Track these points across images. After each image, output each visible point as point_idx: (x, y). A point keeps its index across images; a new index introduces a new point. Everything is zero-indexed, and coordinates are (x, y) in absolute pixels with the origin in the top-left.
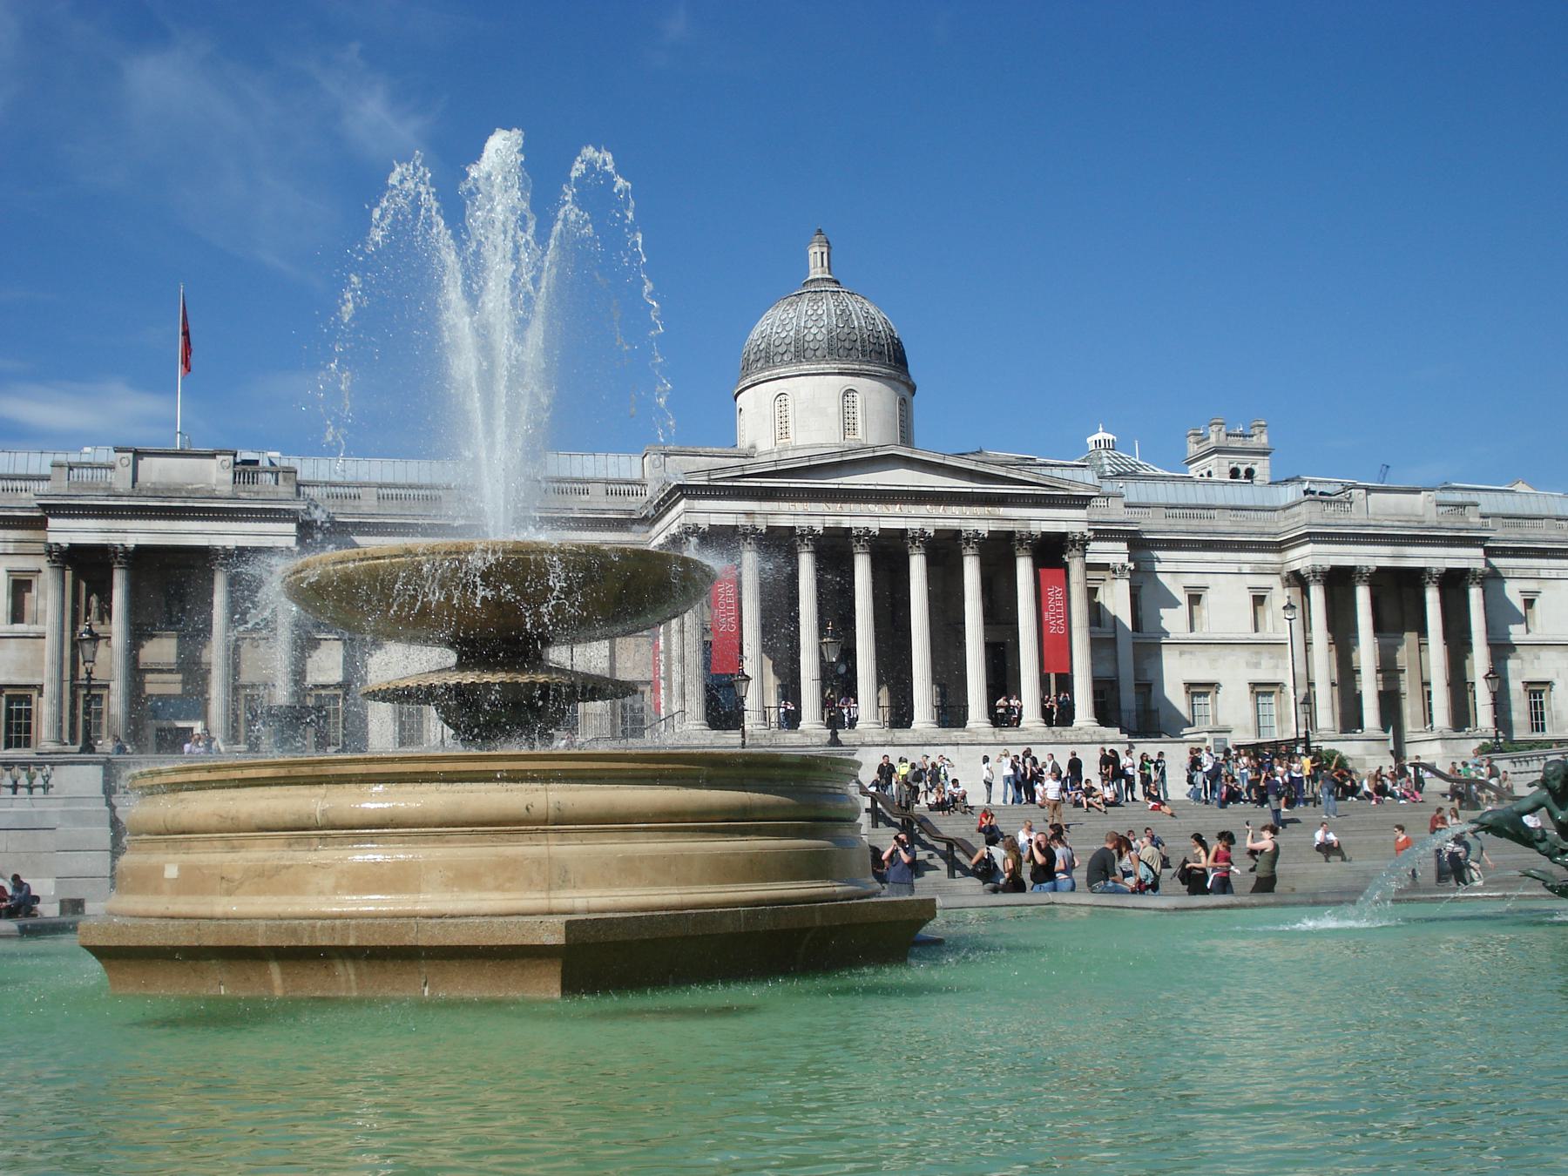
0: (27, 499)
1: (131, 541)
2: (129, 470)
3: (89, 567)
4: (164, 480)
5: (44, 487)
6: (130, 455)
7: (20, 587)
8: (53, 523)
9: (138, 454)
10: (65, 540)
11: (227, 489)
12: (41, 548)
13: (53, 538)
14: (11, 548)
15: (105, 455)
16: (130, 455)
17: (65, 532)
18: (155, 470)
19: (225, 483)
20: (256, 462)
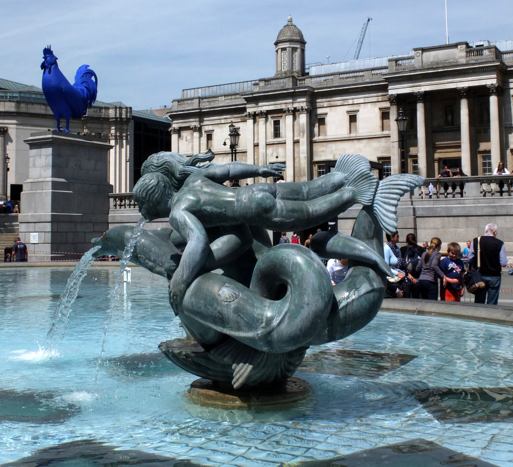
0: (378, 78)
1: (423, 89)
2: (420, 58)
3: (405, 104)
4: (435, 60)
5: (384, 71)
6: (420, 52)
7: (385, 115)
11: (463, 61)
12: (386, 98)
13: (391, 92)
14: (380, 99)
15: (412, 53)
16: (420, 52)
17: (395, 90)
18: (430, 57)
19: (462, 57)
20: (483, 45)
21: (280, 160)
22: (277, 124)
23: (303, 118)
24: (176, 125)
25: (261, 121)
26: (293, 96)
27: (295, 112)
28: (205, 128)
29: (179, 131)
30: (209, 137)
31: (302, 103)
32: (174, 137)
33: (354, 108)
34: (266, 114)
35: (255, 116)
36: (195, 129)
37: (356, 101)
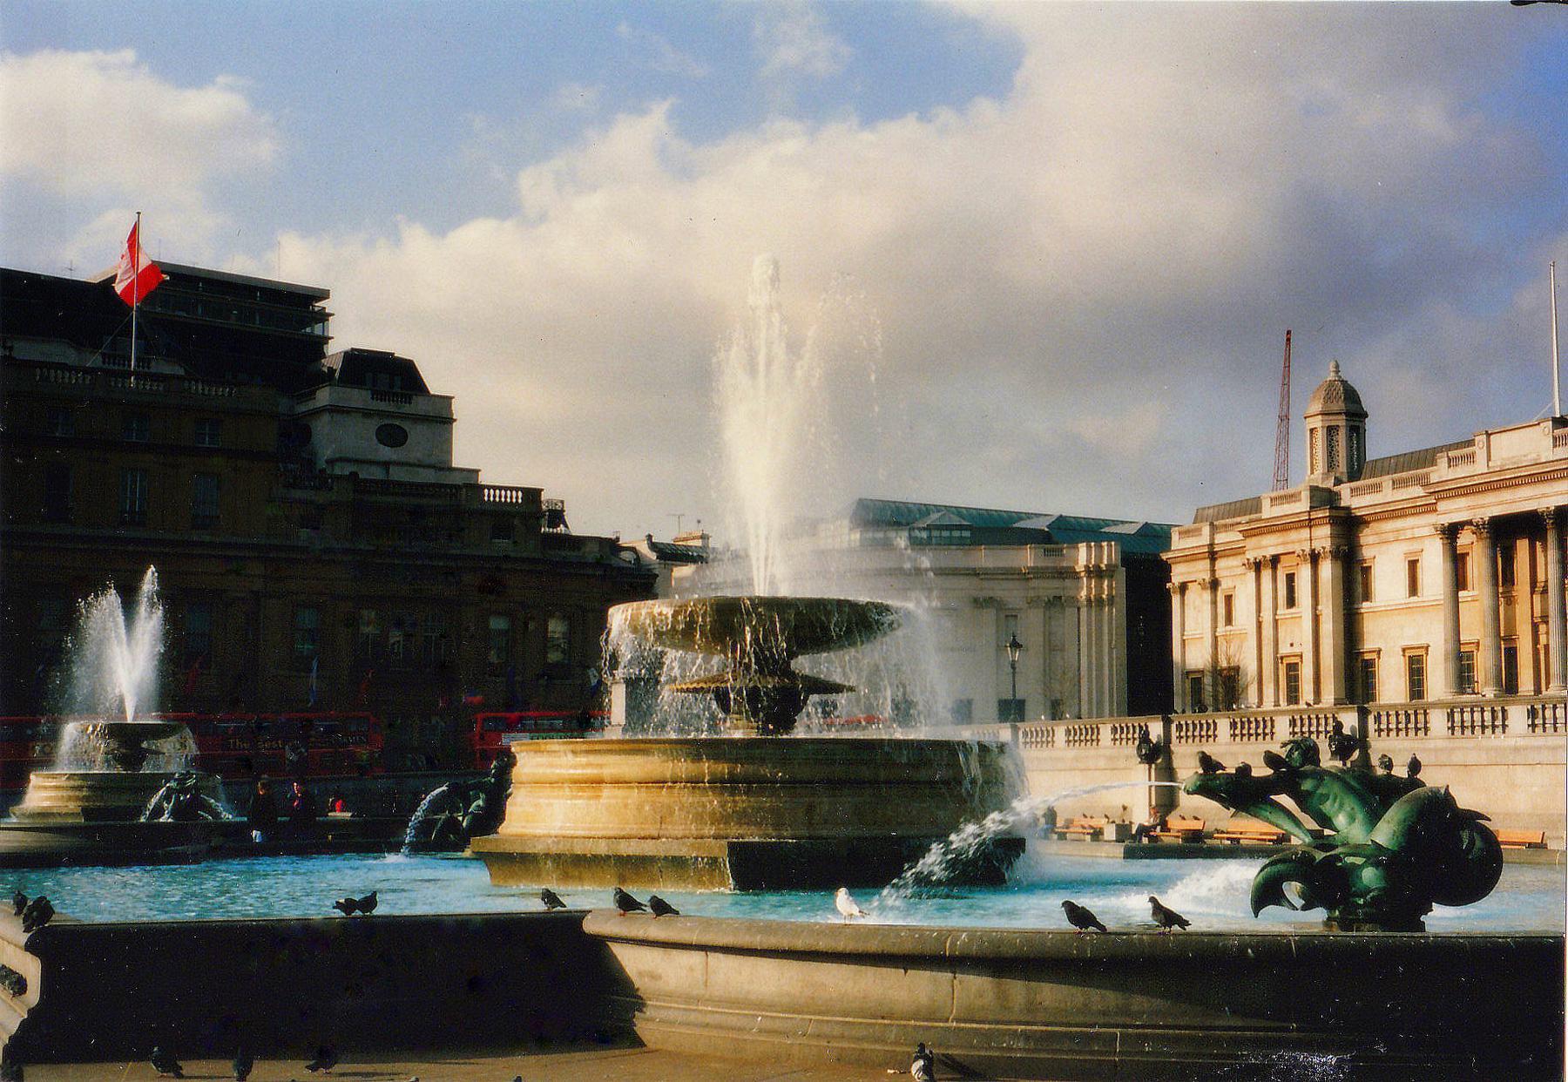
8: (1442, 506)
9: (1488, 435)
10: (1447, 520)
21: (1296, 650)
22: (1290, 578)
23: (1327, 569)
24: (1178, 574)
25: (1266, 574)
26: (1310, 523)
27: (1314, 558)
28: (1225, 585)
29: (1183, 588)
30: (1229, 599)
31: (1323, 537)
32: (1176, 600)
33: (1415, 546)
34: (1275, 560)
35: (1257, 566)
36: (1203, 585)
37: (1417, 533)
